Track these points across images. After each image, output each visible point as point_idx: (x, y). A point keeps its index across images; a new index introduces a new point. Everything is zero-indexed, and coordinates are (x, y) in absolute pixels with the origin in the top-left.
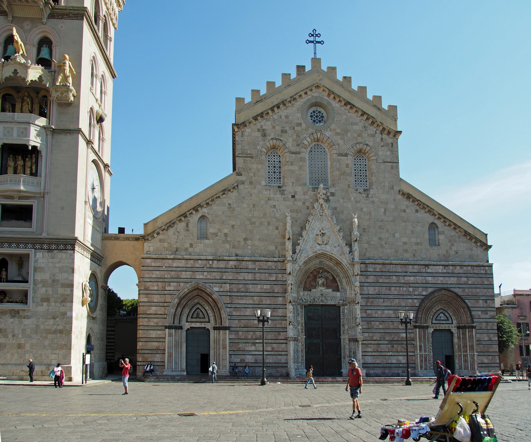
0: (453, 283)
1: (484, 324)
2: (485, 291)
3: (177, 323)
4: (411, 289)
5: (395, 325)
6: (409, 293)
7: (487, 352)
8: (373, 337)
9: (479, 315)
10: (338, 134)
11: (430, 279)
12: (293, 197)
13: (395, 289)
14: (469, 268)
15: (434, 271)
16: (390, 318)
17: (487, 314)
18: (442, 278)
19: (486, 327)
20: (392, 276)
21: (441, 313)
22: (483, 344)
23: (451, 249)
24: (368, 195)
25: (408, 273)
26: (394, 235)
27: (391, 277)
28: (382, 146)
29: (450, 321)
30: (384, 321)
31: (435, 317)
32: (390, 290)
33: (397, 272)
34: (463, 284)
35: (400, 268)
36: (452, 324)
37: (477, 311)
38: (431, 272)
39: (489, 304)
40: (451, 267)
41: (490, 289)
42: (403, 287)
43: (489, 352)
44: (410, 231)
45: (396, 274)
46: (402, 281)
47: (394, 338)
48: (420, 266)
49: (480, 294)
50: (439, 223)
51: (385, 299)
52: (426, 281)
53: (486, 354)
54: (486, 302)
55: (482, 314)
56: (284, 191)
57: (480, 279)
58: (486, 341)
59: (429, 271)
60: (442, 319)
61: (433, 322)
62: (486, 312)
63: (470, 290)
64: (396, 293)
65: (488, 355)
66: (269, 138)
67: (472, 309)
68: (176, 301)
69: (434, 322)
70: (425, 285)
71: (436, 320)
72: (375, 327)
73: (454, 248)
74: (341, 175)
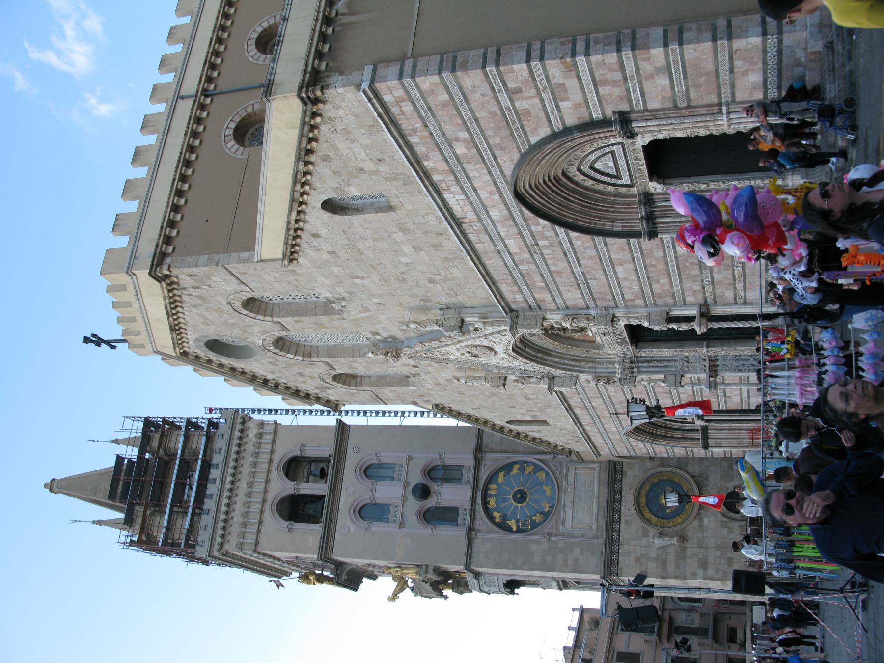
0: (485, 171)
1: (604, 90)
2: (476, 98)
3: (699, 435)
4: (542, 243)
5: (654, 262)
6: (557, 244)
7: (718, 77)
8: (695, 291)
9: (576, 106)
10: (245, 332)
11: (495, 214)
12: (415, 367)
13: (555, 265)
14: (413, 140)
15: (467, 208)
16: (636, 270)
17: (563, 85)
18: (480, 192)
19: (614, 83)
20: (519, 270)
21: (592, 168)
22: (687, 90)
23: (377, 172)
24: (338, 299)
25: (498, 247)
26: (407, 264)
27: (523, 272)
28: (210, 286)
29: (618, 150)
30: (649, 279)
31: (611, 180)
32: (559, 272)
33: (505, 264)
34: (479, 151)
35: (490, 259)
36: (622, 144)
37: (559, 111)
38: (473, 213)
39: (522, 82)
40: (436, 178)
41: (463, 84)
42: (542, 254)
43: (717, 71)
44: (377, 243)
45: (511, 264)
46: (527, 256)
47: (691, 263)
48: (467, 231)
49: (495, 108)
50: (315, 200)
51: (588, 277)
52: (507, 220)
53: (725, 76)
54: (518, 91)
55: (567, 99)
56: (411, 374)
57: (439, 114)
58: (671, 79)
59: (471, 215)
60: (611, 164)
61: (629, 182)
62: (558, 93)
63: (489, 133)
64: (563, 265)
65: (732, 70)
66: (328, 385)
67: (558, 126)
68: (660, 442)
69: (626, 180)
70: (520, 221)
71: (618, 177)
72: (668, 287)
73: (369, 166)
74: (325, 327)
